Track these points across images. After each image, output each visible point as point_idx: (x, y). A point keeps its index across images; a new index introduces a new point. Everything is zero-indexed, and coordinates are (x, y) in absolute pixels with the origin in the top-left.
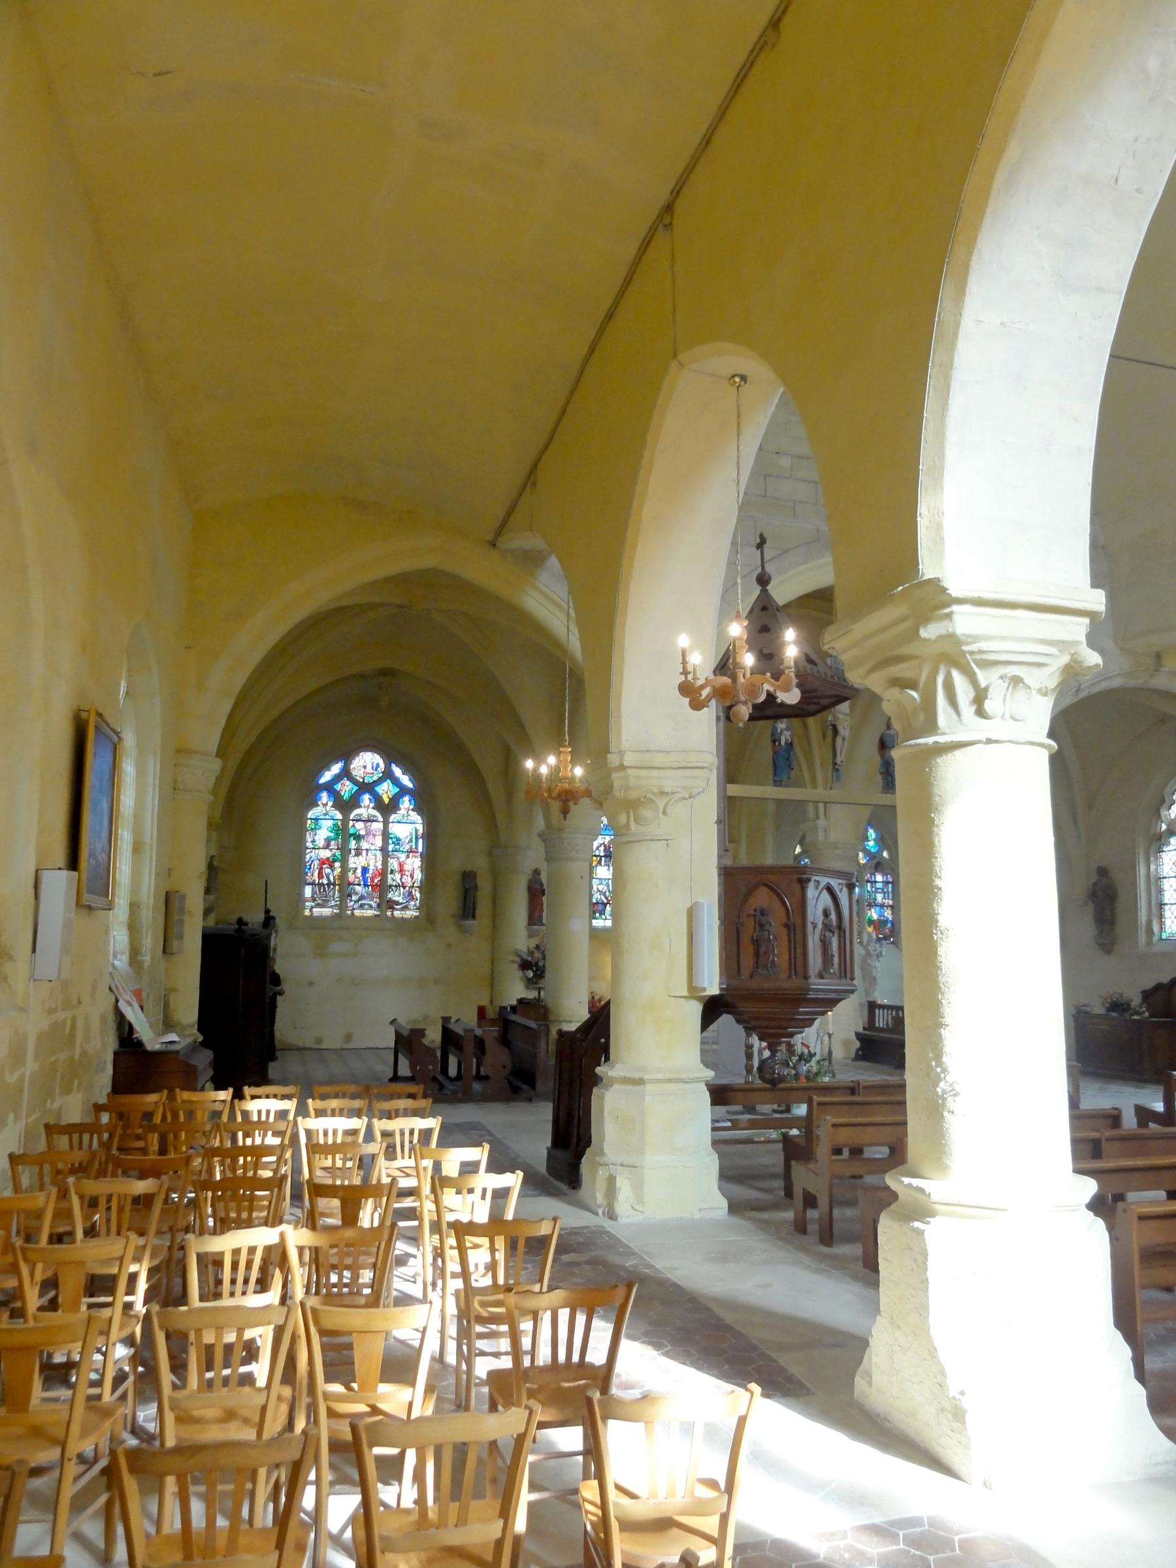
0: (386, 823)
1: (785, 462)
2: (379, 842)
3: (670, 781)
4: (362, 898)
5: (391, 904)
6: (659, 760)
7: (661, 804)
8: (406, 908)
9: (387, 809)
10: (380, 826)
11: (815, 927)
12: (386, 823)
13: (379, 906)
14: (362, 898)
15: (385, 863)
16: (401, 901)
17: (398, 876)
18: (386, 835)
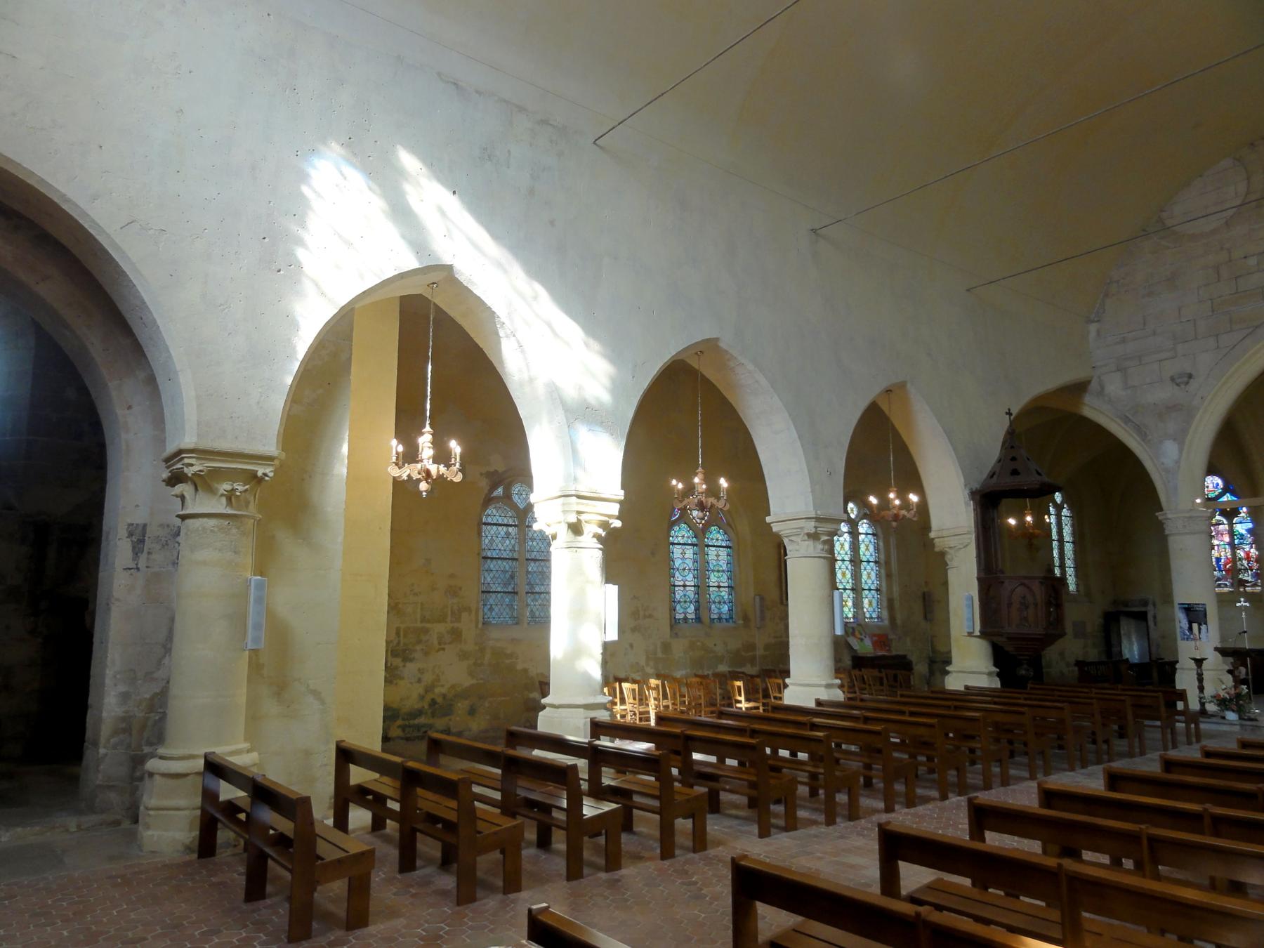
0: (1231, 525)
1: (1252, 261)
2: (1227, 539)
3: (952, 542)
4: (1219, 579)
5: (1243, 583)
6: (945, 534)
7: (951, 551)
8: (1255, 585)
9: (1231, 514)
10: (1227, 527)
11: (1010, 605)
12: (1231, 525)
13: (1232, 585)
14: (1219, 579)
15: (1234, 554)
16: (1250, 579)
17: (1245, 562)
18: (1232, 533)
